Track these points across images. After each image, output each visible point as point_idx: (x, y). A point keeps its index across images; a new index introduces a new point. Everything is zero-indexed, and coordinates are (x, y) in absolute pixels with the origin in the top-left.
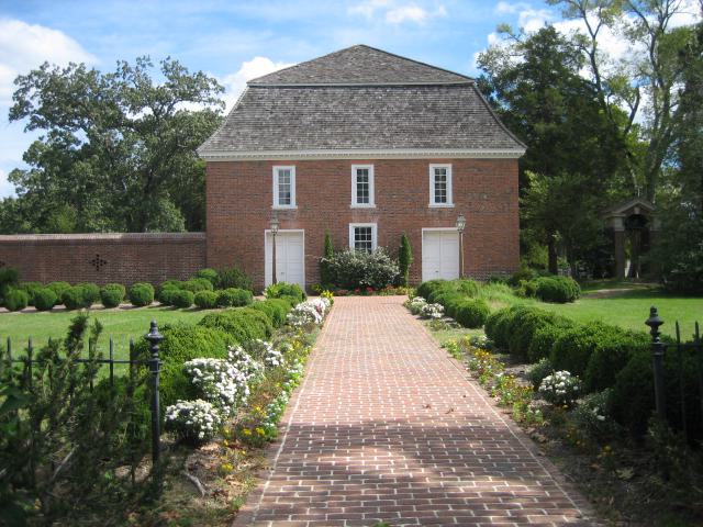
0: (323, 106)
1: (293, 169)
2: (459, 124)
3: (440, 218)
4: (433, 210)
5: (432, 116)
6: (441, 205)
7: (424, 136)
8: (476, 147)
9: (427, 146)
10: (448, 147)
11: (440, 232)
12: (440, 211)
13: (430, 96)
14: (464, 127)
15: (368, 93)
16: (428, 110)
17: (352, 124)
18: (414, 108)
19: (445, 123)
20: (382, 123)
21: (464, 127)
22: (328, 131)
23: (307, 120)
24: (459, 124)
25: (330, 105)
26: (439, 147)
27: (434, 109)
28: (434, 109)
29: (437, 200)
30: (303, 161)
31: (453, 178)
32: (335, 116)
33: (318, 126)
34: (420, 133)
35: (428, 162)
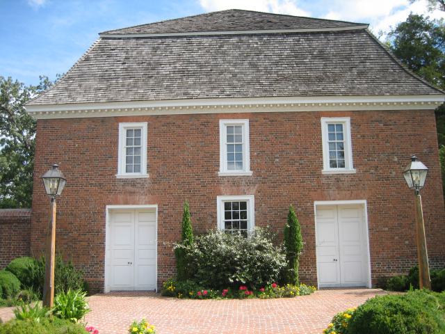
0: (186, 56)
1: (144, 126)
2: (355, 71)
3: (339, 188)
4: (328, 177)
5: (319, 63)
6: (338, 170)
7: (313, 84)
8: (381, 94)
9: (317, 94)
10: (345, 95)
11: (337, 206)
12: (338, 178)
13: (315, 44)
14: (360, 74)
15: (241, 41)
16: (314, 57)
17: (222, 73)
18: (298, 55)
19: (337, 70)
20: (259, 71)
21: (360, 74)
22: (191, 81)
23: (166, 70)
24: (355, 71)
25: (195, 55)
26: (332, 94)
27: (322, 55)
28: (322, 55)
29: (333, 164)
30: (157, 117)
31: (353, 136)
32: (201, 66)
33: (178, 76)
34: (307, 81)
35: (319, 115)
